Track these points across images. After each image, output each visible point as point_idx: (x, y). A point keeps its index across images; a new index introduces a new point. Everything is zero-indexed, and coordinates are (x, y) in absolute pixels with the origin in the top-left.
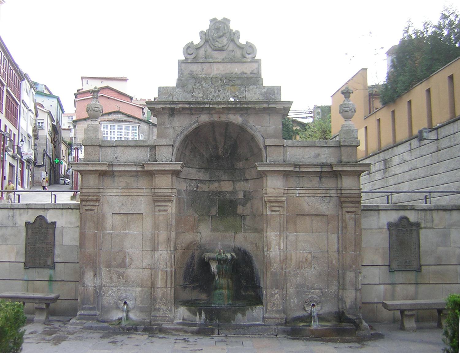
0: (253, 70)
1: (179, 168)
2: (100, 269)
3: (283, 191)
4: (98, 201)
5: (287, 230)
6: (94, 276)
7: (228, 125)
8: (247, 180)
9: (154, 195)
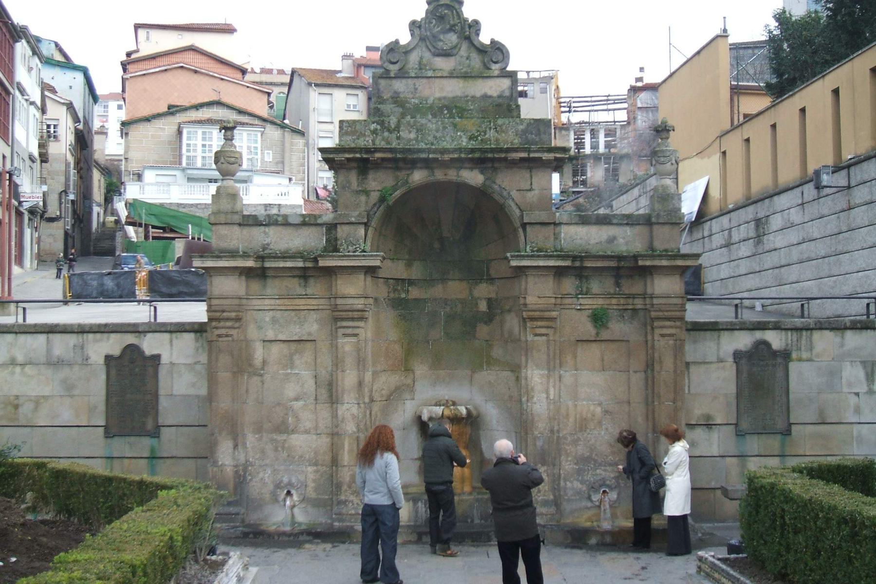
0: (503, 91)
1: (378, 263)
2: (244, 436)
3: (553, 301)
4: (238, 319)
5: (561, 366)
6: (234, 448)
7: (462, 187)
8: (492, 279)
9: (335, 308)
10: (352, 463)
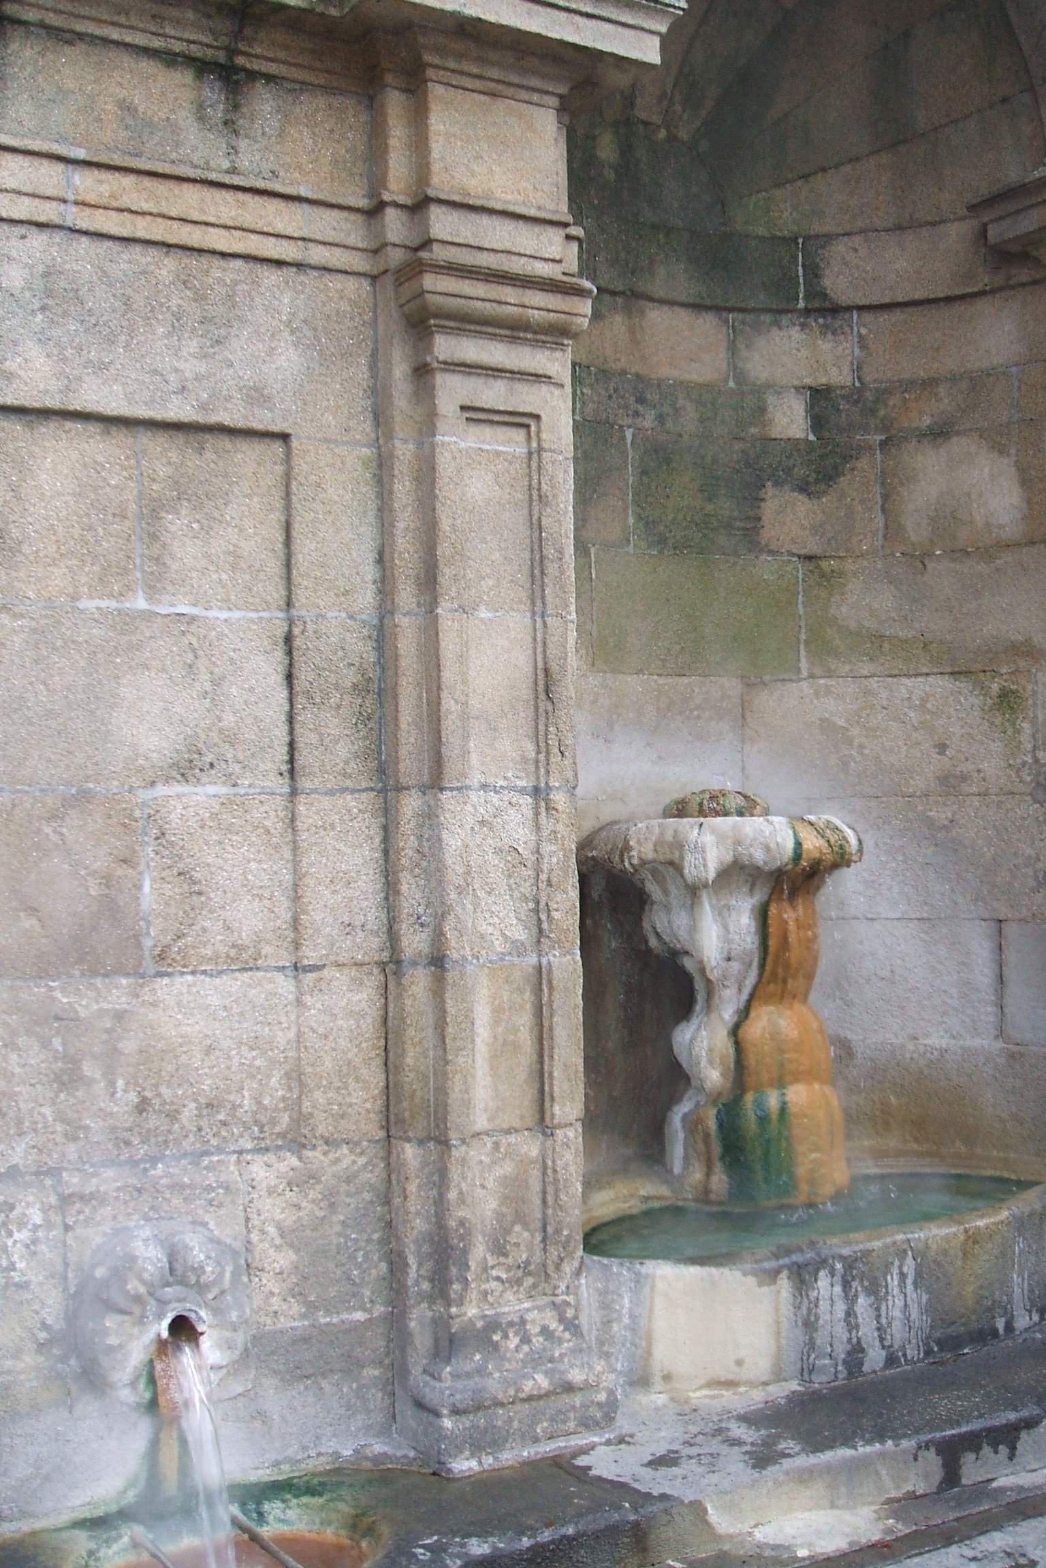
10: (510, 1119)
